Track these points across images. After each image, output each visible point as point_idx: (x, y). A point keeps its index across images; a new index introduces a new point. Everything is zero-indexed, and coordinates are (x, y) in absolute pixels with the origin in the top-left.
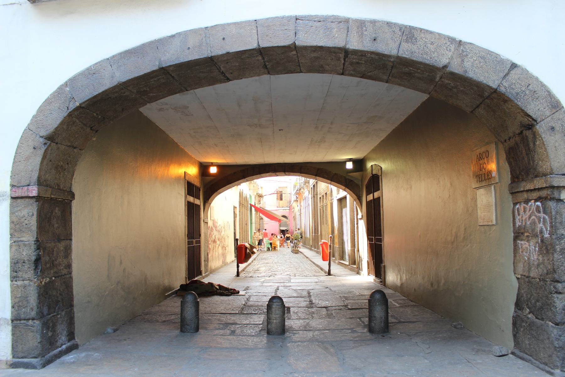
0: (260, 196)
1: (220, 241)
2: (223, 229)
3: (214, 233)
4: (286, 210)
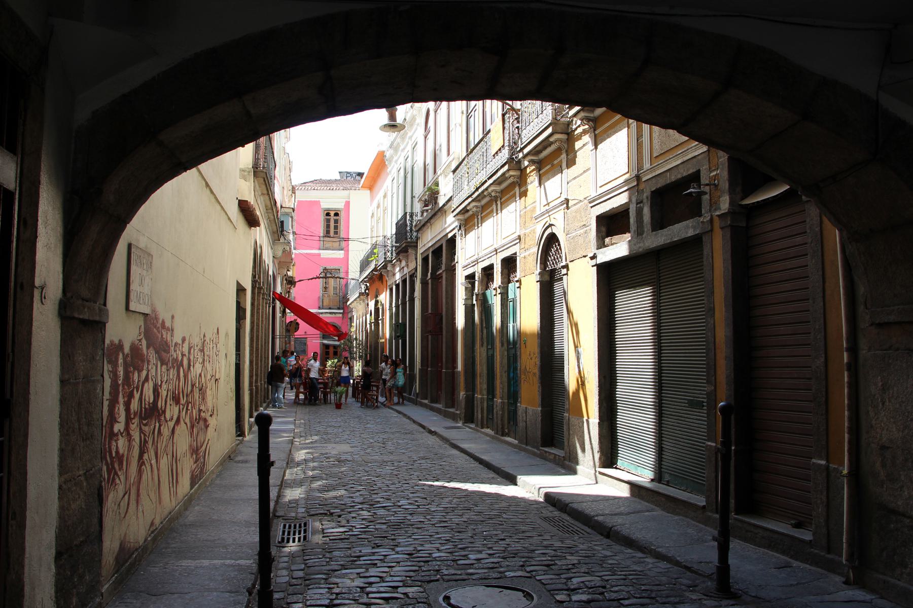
0: (291, 282)
1: (183, 401)
2: (196, 354)
3: (153, 372)
4: (335, 313)
